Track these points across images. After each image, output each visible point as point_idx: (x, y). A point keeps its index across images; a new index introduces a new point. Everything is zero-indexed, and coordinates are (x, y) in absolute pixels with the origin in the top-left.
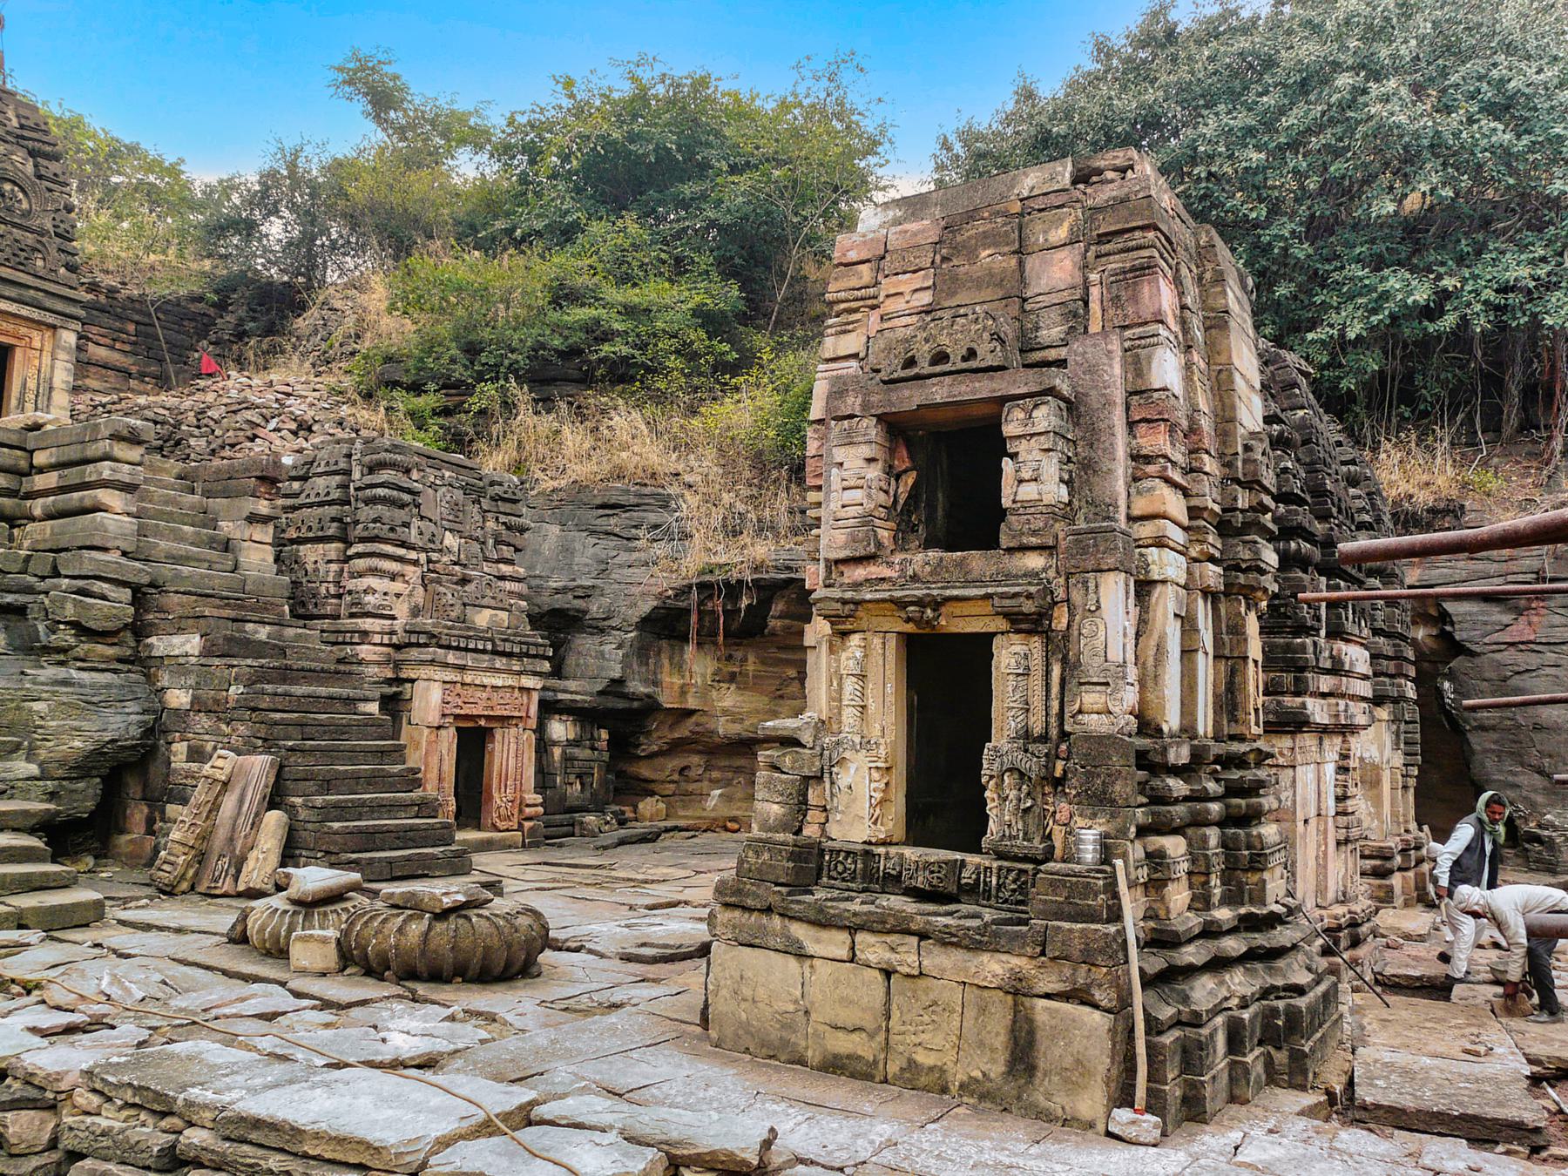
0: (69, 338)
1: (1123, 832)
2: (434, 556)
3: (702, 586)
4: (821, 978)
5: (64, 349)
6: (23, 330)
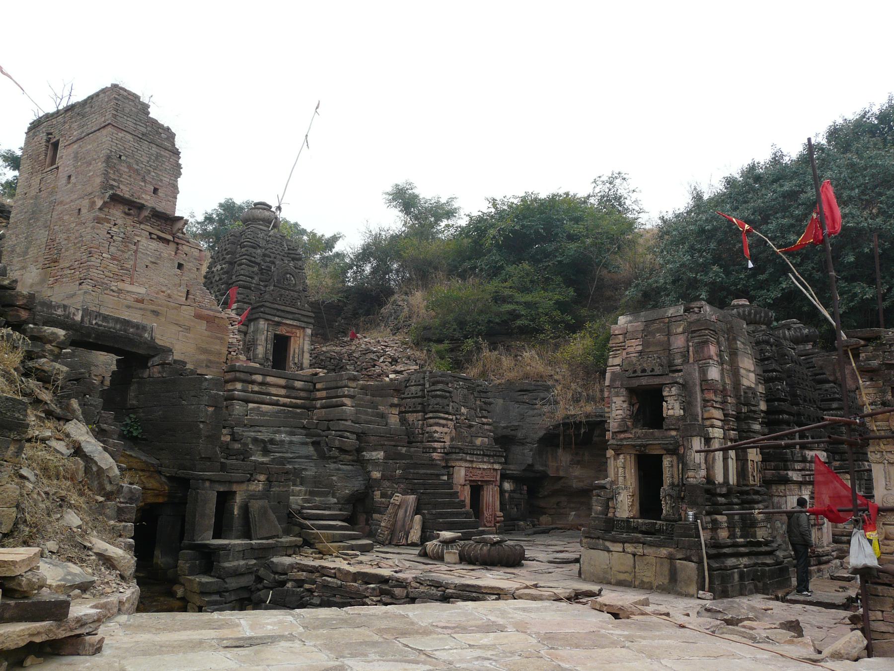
0: (309, 331)
1: (701, 513)
2: (458, 417)
3: (564, 424)
4: (616, 557)
6: (294, 330)
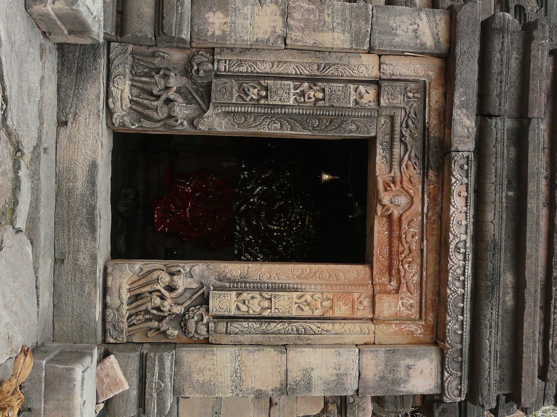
5: (391, 367)
6: (411, 273)
